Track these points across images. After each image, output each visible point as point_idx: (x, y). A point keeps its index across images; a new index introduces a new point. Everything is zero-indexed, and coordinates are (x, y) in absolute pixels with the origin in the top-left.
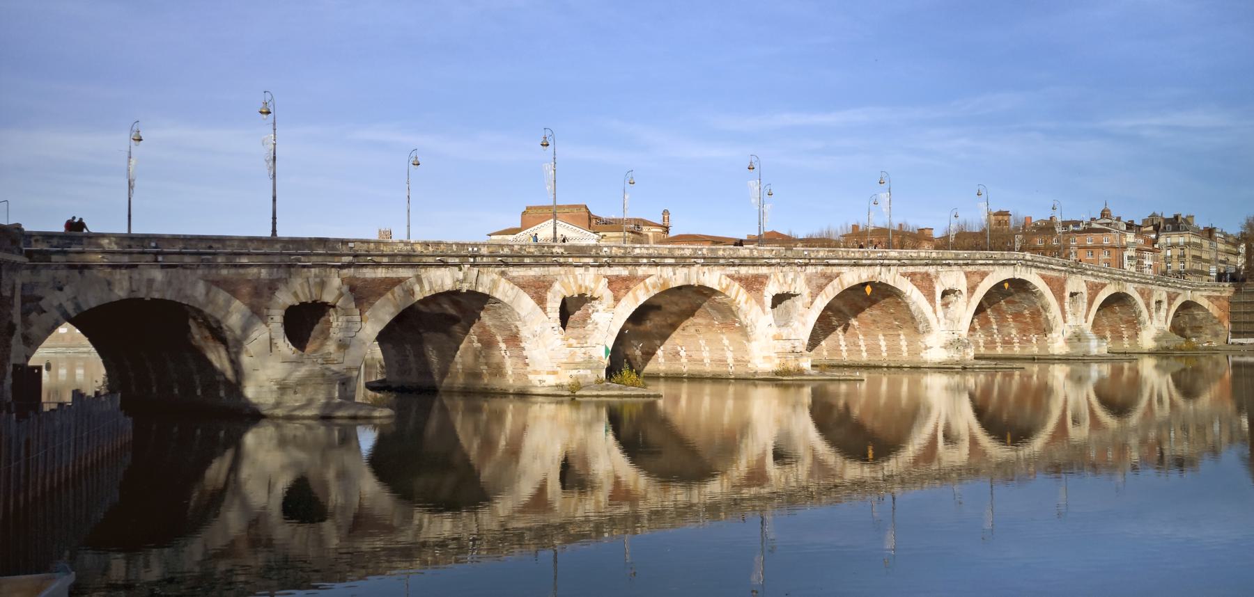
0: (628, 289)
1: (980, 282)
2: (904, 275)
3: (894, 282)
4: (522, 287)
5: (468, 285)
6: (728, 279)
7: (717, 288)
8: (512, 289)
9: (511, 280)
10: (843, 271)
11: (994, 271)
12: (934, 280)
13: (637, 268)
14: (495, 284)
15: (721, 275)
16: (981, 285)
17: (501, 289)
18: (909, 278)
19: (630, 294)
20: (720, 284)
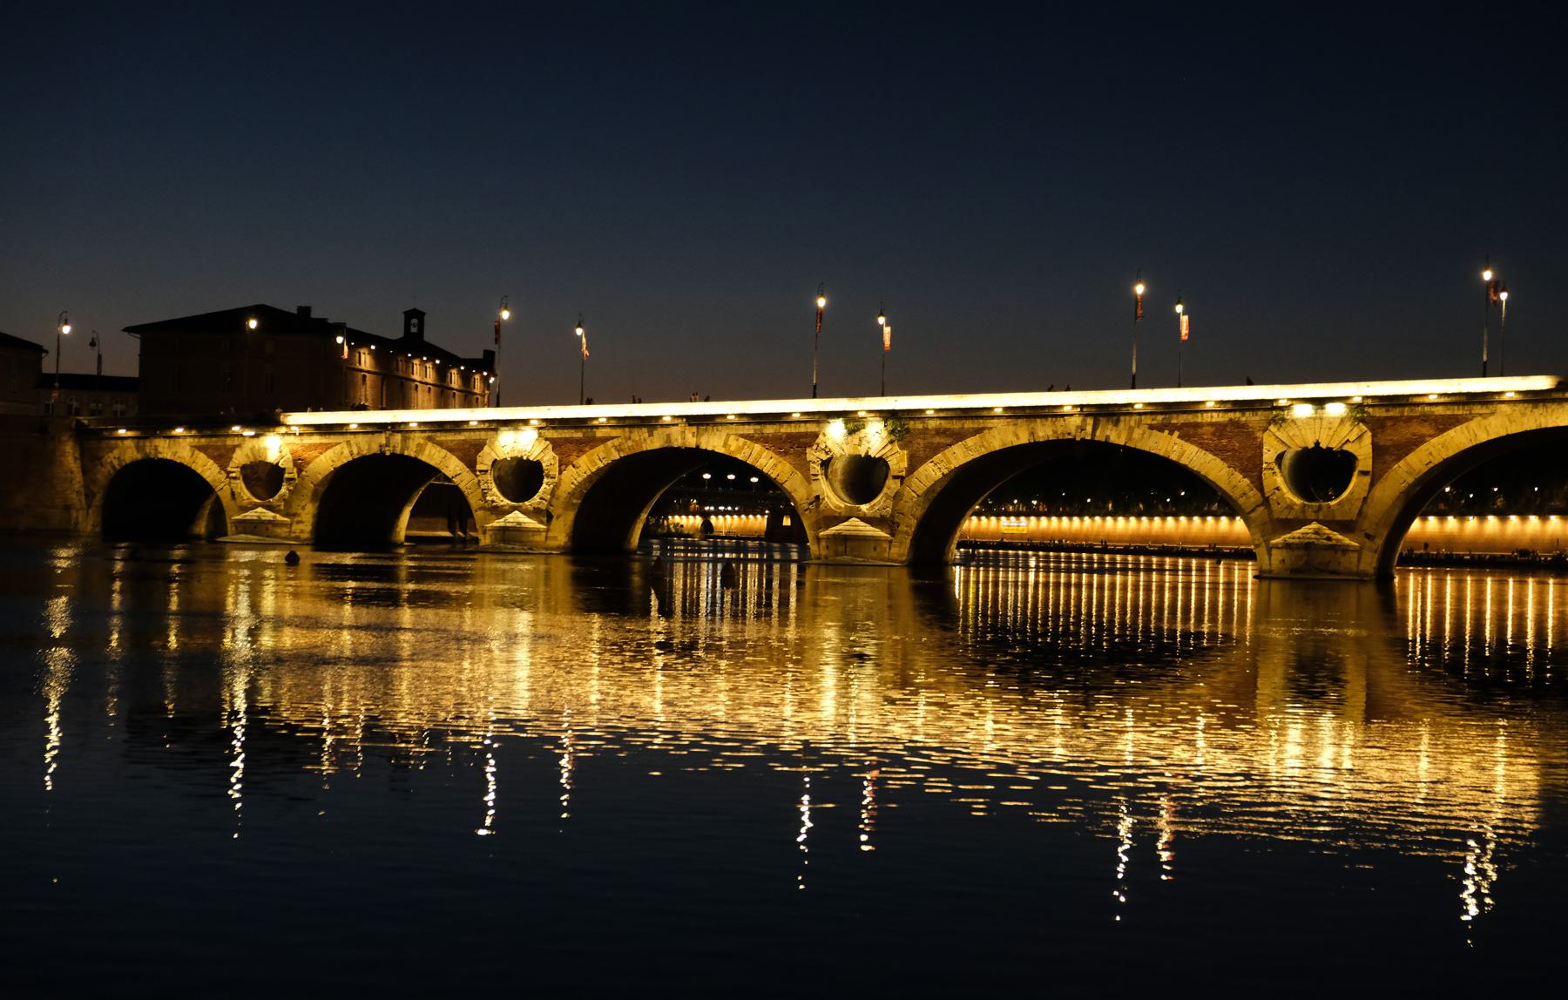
0: (582, 452)
1: (1432, 436)
2: (1151, 427)
3: (1130, 438)
4: (451, 450)
5: (391, 449)
6: (742, 440)
7: (722, 451)
8: (439, 452)
9: (440, 444)
10: (990, 425)
11: (1493, 413)
12: (1259, 434)
13: (595, 430)
14: (421, 447)
15: (728, 435)
16: (1434, 441)
17: (427, 452)
18: (1177, 433)
19: (584, 458)
20: (725, 444)
